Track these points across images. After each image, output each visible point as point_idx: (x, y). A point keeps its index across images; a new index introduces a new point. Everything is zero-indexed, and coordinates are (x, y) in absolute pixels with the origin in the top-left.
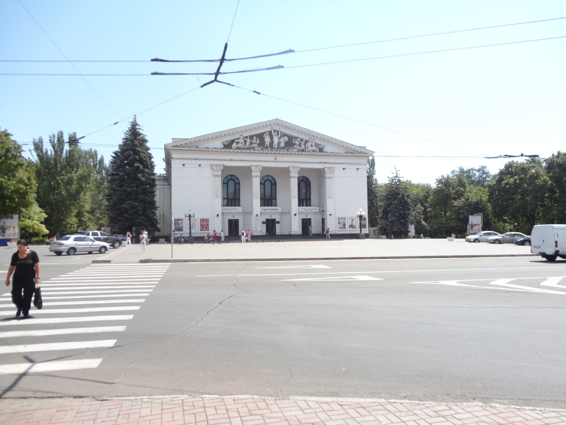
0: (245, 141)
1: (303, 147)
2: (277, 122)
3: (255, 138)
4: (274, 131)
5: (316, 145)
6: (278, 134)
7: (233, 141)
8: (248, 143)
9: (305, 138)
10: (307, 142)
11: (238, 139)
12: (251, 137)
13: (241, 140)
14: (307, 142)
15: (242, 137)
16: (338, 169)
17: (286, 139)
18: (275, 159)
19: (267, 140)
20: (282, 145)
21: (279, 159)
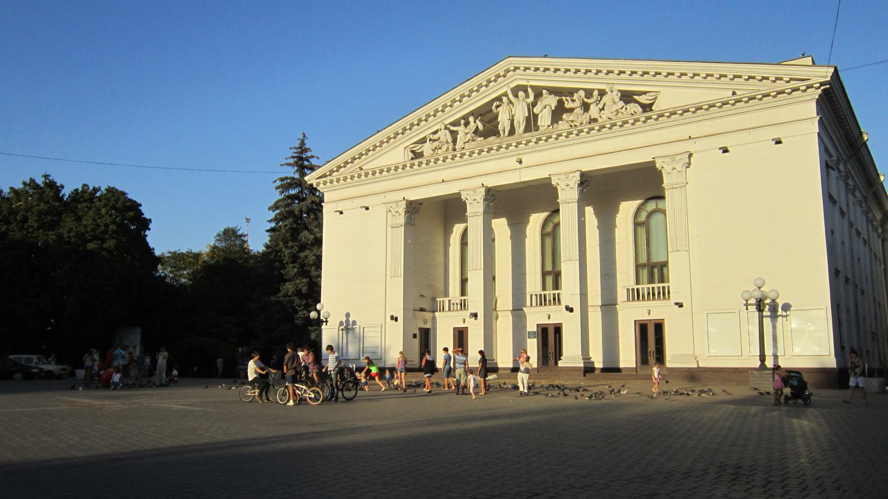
0: (454, 134)
3: (471, 119)
4: (515, 91)
5: (627, 97)
6: (527, 96)
7: (423, 141)
10: (602, 93)
11: (436, 132)
13: (444, 135)
14: (602, 93)
15: (443, 127)
16: (706, 154)
17: (551, 101)
20: (544, 119)
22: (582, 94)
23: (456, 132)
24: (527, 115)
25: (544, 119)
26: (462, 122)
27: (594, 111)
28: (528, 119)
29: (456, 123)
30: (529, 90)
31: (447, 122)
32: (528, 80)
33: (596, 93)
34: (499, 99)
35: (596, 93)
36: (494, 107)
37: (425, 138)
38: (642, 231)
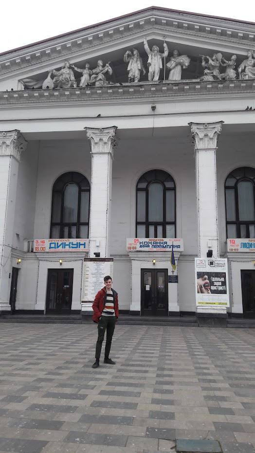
0: (78, 76)
1: (231, 73)
2: (153, 17)
3: (100, 63)
4: (151, 43)
6: (162, 51)
7: (44, 76)
8: (84, 79)
9: (236, 51)
10: (240, 59)
11: (58, 70)
12: (92, 64)
13: (67, 74)
14: (240, 59)
17: (186, 61)
18: (154, 108)
19: (134, 67)
20: (176, 75)
21: (161, 108)
22: (220, 56)
23: (81, 75)
24: (161, 67)
25: (176, 75)
26: (87, 66)
27: (231, 73)
28: (161, 71)
29: (81, 65)
30: (165, 45)
31: (72, 62)
32: (164, 36)
33: (234, 57)
34: (131, 49)
35: (234, 57)
36: (126, 56)
37: (47, 73)
38: (231, 193)
